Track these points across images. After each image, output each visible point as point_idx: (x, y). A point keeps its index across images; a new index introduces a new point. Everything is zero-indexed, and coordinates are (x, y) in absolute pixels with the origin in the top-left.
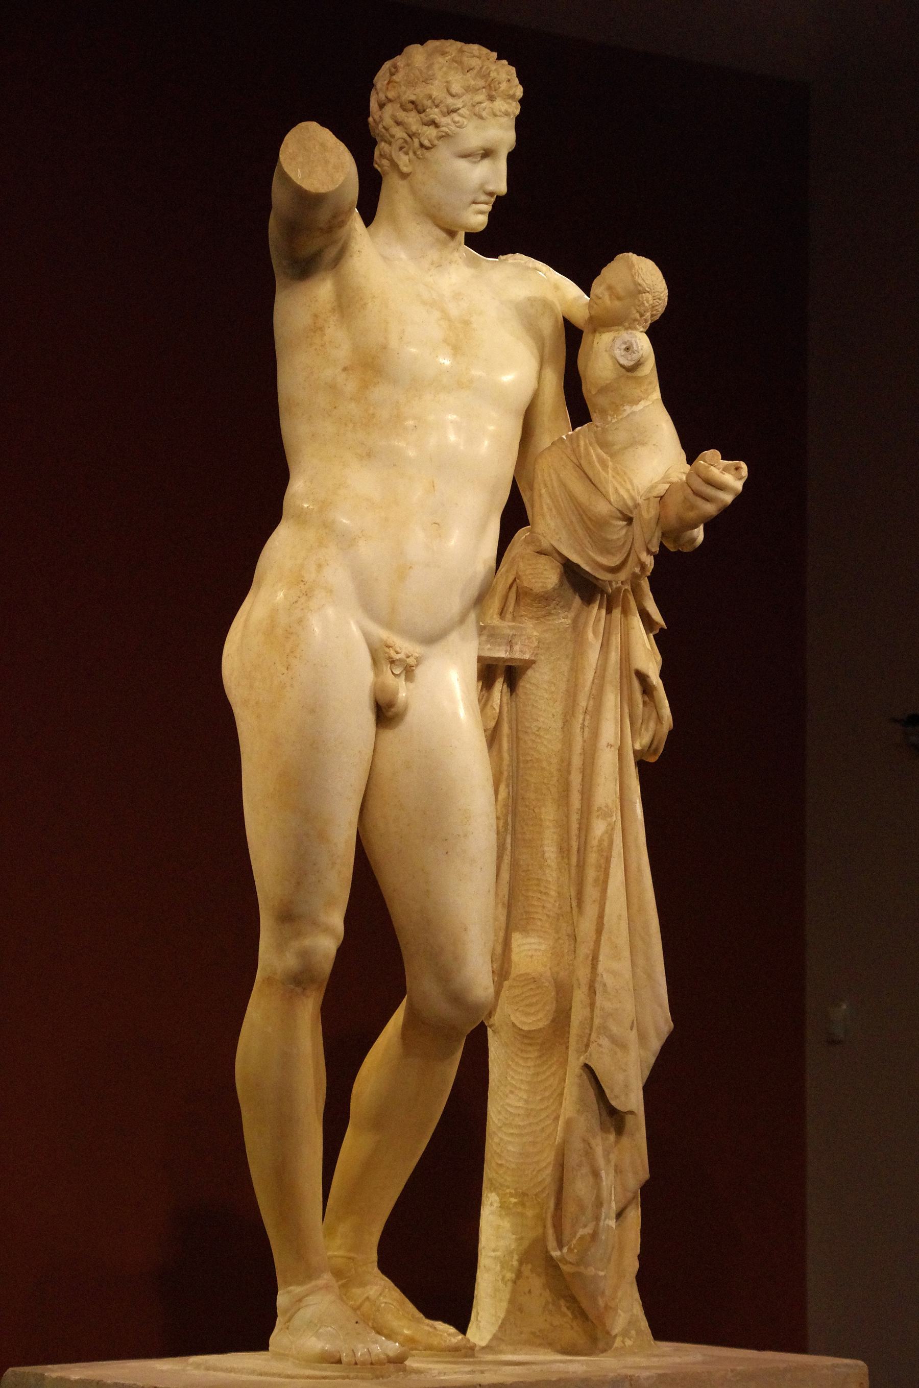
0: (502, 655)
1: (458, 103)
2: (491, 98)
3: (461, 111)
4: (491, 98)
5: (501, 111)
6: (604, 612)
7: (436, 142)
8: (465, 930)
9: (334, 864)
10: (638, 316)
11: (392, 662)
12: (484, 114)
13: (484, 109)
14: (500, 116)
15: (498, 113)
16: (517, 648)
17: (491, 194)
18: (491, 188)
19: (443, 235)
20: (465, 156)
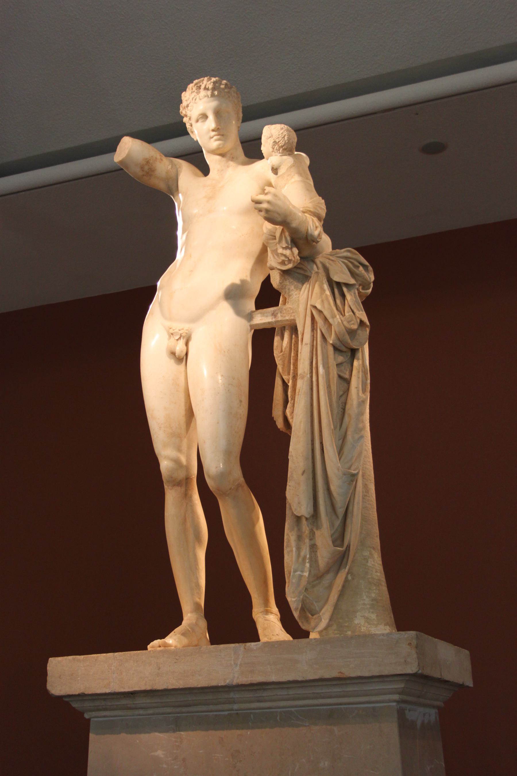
2: (198, 93)
6: (308, 286)
7: (190, 122)
8: (205, 442)
9: (160, 427)
11: (172, 334)
13: (195, 100)
15: (201, 98)
16: (279, 315)
17: (213, 130)
19: (218, 157)
20: (197, 121)
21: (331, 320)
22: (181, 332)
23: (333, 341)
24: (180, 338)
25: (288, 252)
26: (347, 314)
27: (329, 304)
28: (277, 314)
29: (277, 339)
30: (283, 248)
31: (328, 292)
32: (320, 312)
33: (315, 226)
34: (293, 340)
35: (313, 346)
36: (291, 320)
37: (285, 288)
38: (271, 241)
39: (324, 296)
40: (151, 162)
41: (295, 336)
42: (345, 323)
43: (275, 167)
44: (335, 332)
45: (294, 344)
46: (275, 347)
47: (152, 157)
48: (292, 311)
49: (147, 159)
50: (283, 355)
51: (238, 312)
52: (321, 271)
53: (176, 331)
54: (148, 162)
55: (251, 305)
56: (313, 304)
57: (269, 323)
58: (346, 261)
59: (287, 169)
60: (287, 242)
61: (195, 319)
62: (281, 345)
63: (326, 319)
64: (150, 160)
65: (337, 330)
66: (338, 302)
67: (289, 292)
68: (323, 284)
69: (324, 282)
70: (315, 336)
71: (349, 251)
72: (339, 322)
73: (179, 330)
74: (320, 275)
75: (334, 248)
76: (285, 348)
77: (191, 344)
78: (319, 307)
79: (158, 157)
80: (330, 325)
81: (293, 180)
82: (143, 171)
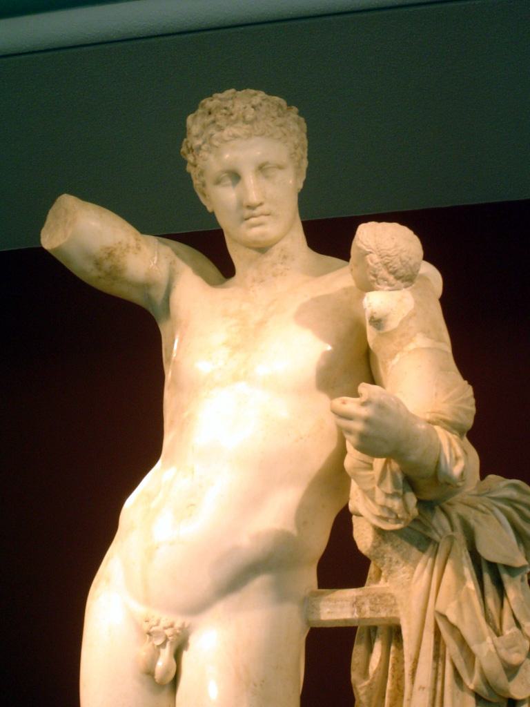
0: (348, 616)
1: (198, 142)
2: (221, 129)
3: (203, 147)
4: (221, 129)
5: (229, 136)
6: (430, 560)
10: (373, 278)
12: (216, 143)
14: (231, 140)
15: (227, 138)
16: (367, 607)
18: (245, 203)
19: (254, 253)
20: (218, 182)
21: (475, 648)
22: (168, 632)
23: (475, 685)
24: (163, 645)
25: (396, 504)
26: (507, 632)
27: (473, 611)
28: (363, 604)
29: (358, 650)
30: (387, 495)
31: (471, 585)
32: (453, 628)
33: (454, 456)
34: (391, 656)
35: (435, 690)
36: (390, 619)
37: (383, 557)
38: (363, 473)
39: (463, 592)
40: (117, 253)
41: (396, 646)
42: (503, 652)
43: (377, 317)
44: (481, 669)
45: (394, 665)
46: (353, 666)
47: (120, 243)
48: (393, 602)
49: (108, 248)
50: (370, 684)
51: (281, 594)
52: (459, 534)
53: (160, 628)
54: (110, 254)
55: (310, 577)
56: (441, 610)
57: (346, 621)
58: (509, 509)
59: (401, 322)
60: (395, 484)
61: (199, 608)
62: (368, 664)
63: (463, 643)
64: (115, 249)
65: (486, 666)
66: (490, 601)
67: (391, 565)
68: (461, 564)
69: (464, 559)
70: (440, 671)
71: (516, 487)
72: (490, 651)
73: (165, 628)
74: (456, 543)
75: (483, 474)
76: (375, 673)
77: (186, 657)
78: (453, 618)
79: (132, 243)
80: (470, 656)
81: (411, 346)
82: (100, 269)
